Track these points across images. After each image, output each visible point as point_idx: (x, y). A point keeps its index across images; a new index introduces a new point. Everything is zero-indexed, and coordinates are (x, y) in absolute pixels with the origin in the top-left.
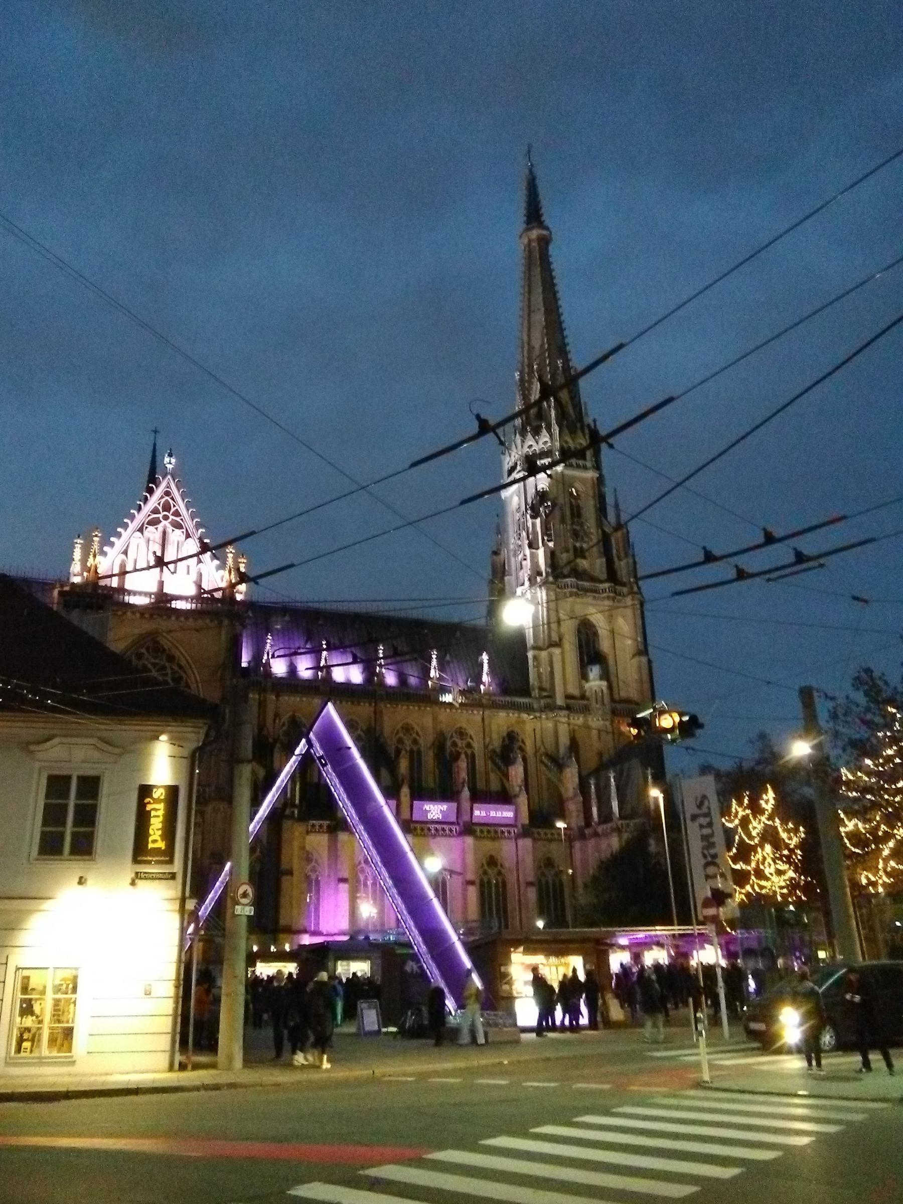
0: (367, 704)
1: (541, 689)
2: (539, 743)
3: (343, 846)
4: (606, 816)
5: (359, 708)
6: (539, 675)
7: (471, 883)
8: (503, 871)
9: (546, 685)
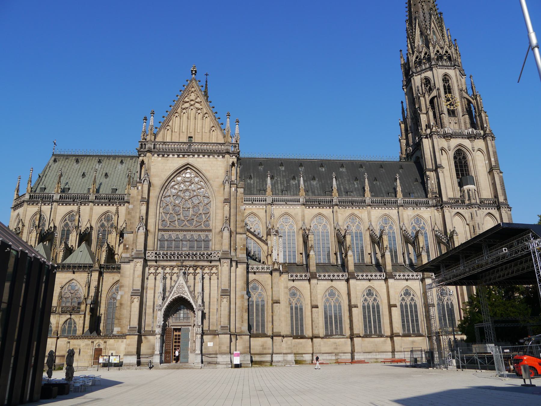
0: (328, 208)
2: (433, 224)
3: (314, 287)
7: (395, 306)
8: (415, 298)
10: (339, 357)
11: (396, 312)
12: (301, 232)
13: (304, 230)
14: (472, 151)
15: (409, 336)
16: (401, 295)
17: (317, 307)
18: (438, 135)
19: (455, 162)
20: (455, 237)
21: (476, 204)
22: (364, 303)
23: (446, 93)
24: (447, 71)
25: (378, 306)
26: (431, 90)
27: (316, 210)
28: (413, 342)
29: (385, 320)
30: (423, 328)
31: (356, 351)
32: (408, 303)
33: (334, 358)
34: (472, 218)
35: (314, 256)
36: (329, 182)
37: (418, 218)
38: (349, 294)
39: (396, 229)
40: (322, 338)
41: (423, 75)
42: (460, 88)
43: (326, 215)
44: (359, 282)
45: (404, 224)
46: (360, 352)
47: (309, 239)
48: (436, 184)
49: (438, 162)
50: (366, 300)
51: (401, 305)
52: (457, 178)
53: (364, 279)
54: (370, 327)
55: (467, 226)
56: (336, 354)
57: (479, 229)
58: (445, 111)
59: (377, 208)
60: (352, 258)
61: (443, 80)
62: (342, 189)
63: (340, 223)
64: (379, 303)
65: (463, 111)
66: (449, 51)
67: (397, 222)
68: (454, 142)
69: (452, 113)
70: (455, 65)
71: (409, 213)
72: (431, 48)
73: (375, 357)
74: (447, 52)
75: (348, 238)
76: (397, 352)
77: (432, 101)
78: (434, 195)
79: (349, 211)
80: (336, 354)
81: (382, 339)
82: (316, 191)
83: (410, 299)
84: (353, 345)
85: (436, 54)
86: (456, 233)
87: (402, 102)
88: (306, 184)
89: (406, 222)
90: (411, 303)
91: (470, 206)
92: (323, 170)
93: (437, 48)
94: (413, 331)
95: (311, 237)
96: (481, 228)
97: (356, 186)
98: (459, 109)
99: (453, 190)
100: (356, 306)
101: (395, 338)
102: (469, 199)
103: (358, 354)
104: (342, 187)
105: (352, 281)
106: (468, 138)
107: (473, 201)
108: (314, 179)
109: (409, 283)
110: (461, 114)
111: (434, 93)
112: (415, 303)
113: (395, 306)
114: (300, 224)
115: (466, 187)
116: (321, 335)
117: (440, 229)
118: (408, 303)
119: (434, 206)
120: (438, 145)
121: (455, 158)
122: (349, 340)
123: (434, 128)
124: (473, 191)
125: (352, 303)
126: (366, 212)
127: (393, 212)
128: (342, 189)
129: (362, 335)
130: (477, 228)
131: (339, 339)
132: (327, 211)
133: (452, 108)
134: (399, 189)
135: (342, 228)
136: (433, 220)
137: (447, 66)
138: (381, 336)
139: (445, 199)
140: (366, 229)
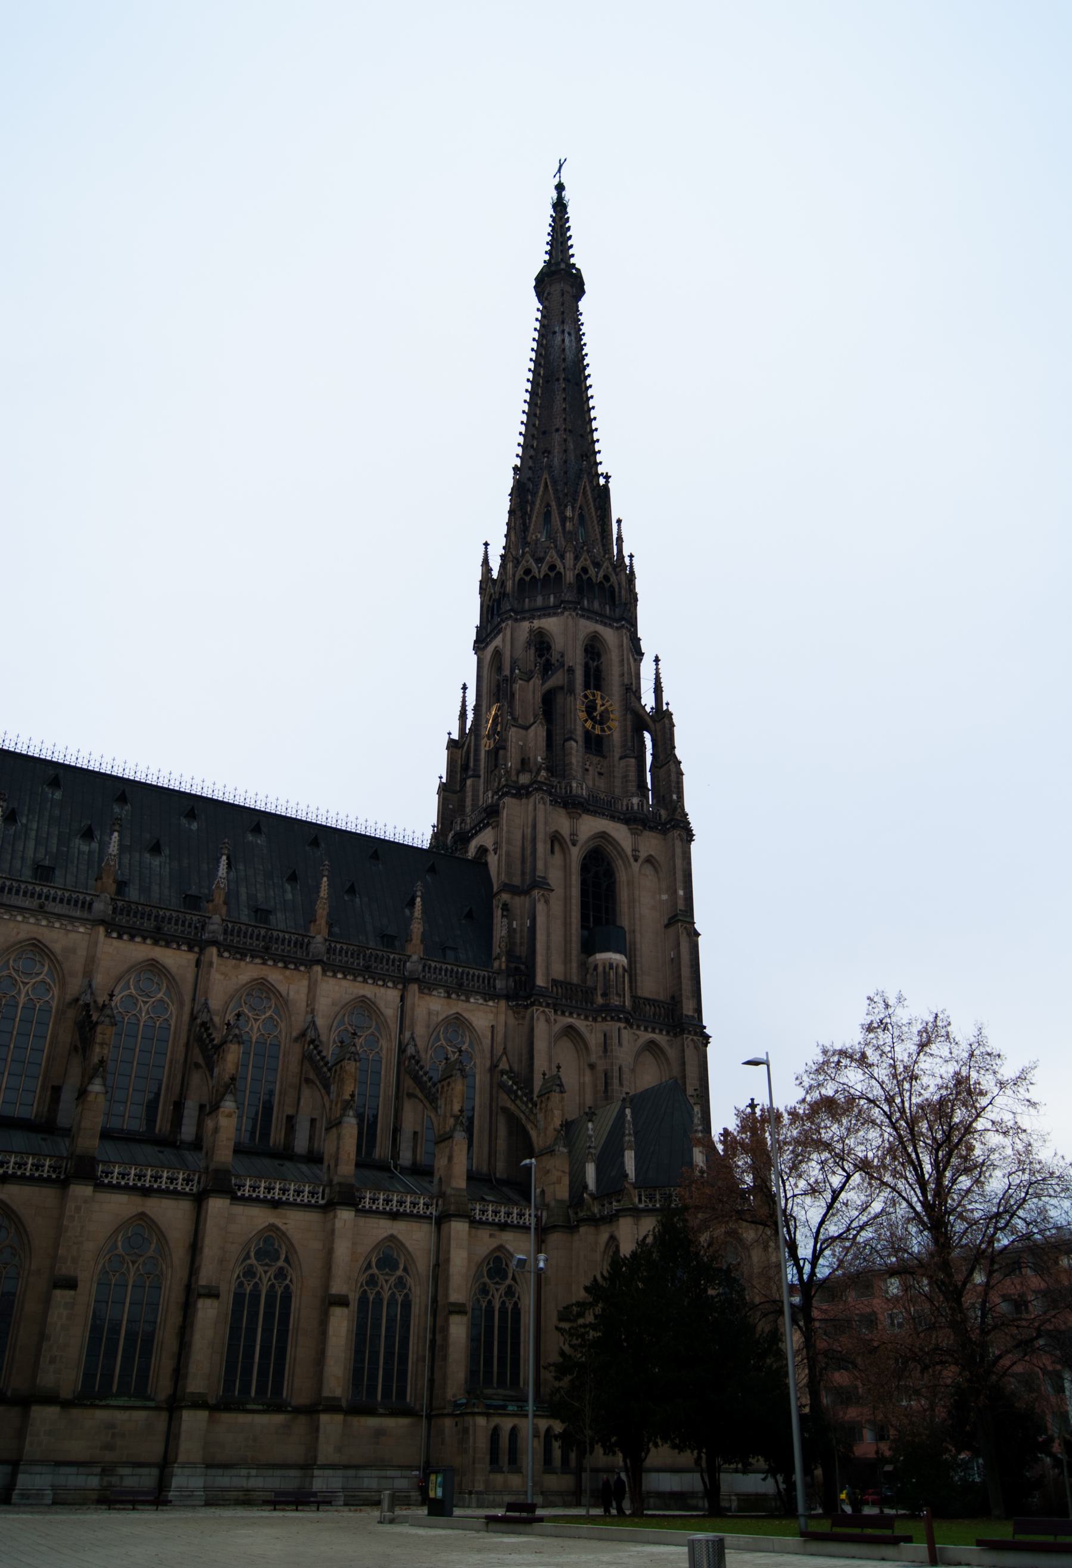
1: (510, 954)
2: (499, 1050)
3: (78, 1209)
4: (612, 1184)
5: (169, 952)
6: (511, 931)
7: (342, 1301)
8: (410, 1281)
9: (521, 951)
10: (115, 1480)
11: (341, 1325)
12: (71, 1014)
13: (87, 1005)
14: (632, 860)
15: (371, 1412)
16: (369, 1266)
17: (71, 1284)
18: (550, 794)
19: (584, 883)
20: (555, 1097)
21: (621, 1009)
22: (241, 1285)
23: (587, 686)
24: (600, 628)
25: (287, 1297)
26: (547, 669)
27: (140, 951)
28: (379, 1433)
29: (300, 1350)
30: (415, 1389)
31: (181, 1458)
32: (386, 1296)
33: (94, 1482)
34: (605, 1051)
35: (101, 1098)
36: (205, 867)
37: (458, 1023)
38: (195, 1248)
39: (387, 1047)
40: (66, 1404)
41: (536, 623)
42: (626, 681)
43: (174, 970)
44: (239, 1209)
45: (413, 1038)
46: (192, 1465)
47: (99, 1038)
48: (525, 934)
49: (540, 872)
50: (250, 1273)
51: (363, 1300)
52: (583, 927)
53: (257, 1200)
54: (247, 1371)
55: (588, 1072)
56: (107, 1470)
57: (621, 1084)
58: (579, 734)
59: (340, 976)
60: (234, 1121)
61: (586, 650)
62: (243, 897)
63: (215, 1003)
64: (293, 1288)
65: (624, 745)
66: (613, 578)
67: (394, 1027)
68: (590, 826)
69: (595, 744)
70: (623, 619)
71: (431, 1007)
72: (569, 556)
73: (243, 1483)
74: (606, 578)
75: (233, 1054)
76: (323, 1467)
77: (548, 700)
78: (513, 965)
79: (249, 971)
80: (107, 1470)
81: (279, 1419)
82: (155, 888)
83: (392, 1280)
84: (171, 1437)
85: (578, 575)
86: (561, 1085)
87: (464, 688)
88: (126, 861)
89: (420, 1031)
90: (393, 1294)
91: (608, 1012)
92: (194, 826)
93: (585, 561)
94: (386, 1394)
95: (105, 1033)
96: (625, 1083)
97: (289, 896)
98: (616, 737)
99: (567, 961)
100: (213, 1294)
101: (324, 1418)
102: (604, 995)
103: (187, 1471)
104: (243, 890)
105: (216, 1205)
106: (626, 821)
107: (616, 1001)
108: (156, 849)
109: (399, 1228)
110: (617, 753)
111: (557, 679)
112: (407, 1295)
113: (342, 1301)
114: (75, 985)
115: (602, 957)
116: (66, 1393)
117: (516, 1067)
118: (386, 1296)
119: (508, 998)
120: (546, 823)
121: (584, 868)
122: (164, 1415)
123: (543, 773)
124: (621, 970)
125: (203, 1282)
126: (305, 983)
127: (387, 997)
128: (243, 897)
129: (212, 1401)
130: (616, 1081)
131: (128, 1413)
132: (176, 960)
133: (597, 731)
134: (417, 928)
135: (216, 1019)
136: (499, 1038)
137: (600, 615)
138: (276, 1407)
139: (540, 981)
140: (295, 1034)
